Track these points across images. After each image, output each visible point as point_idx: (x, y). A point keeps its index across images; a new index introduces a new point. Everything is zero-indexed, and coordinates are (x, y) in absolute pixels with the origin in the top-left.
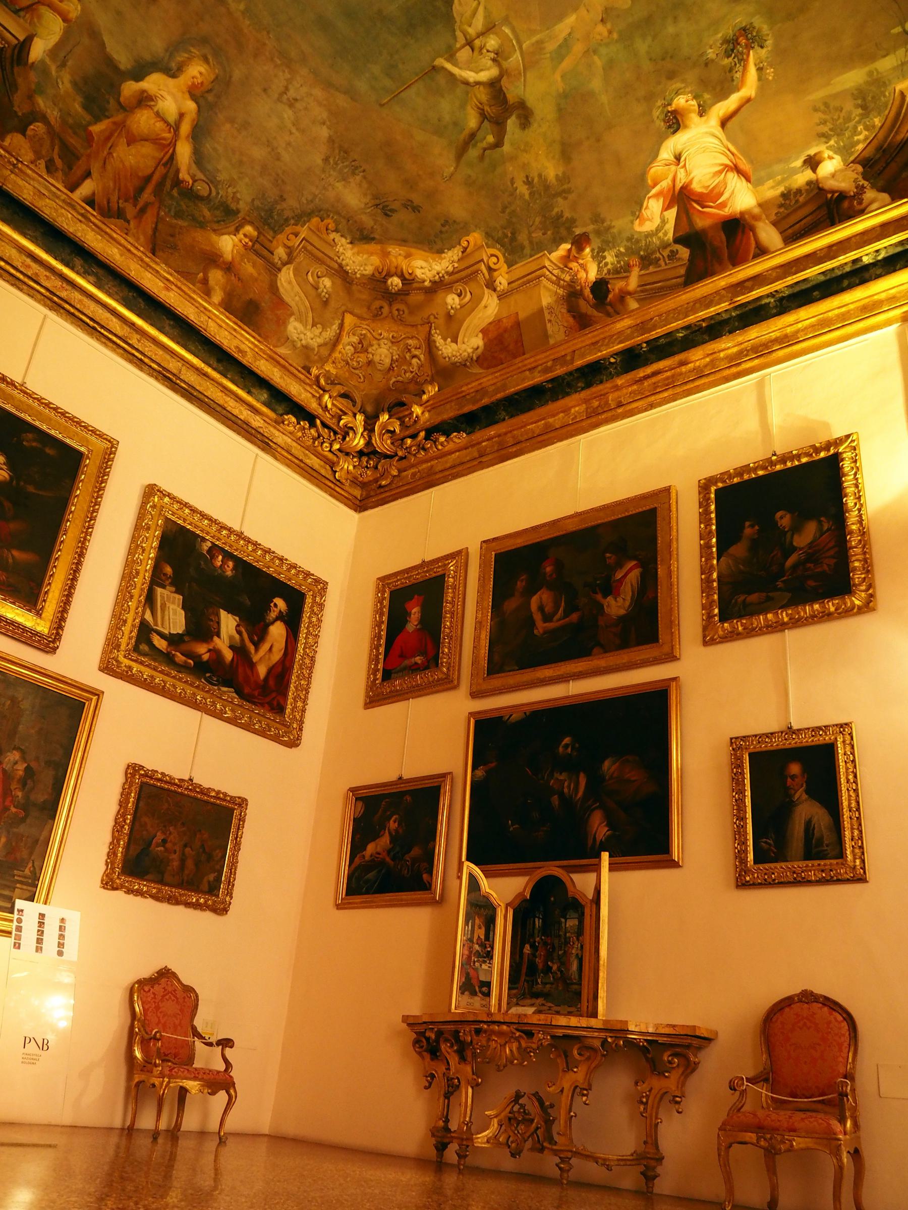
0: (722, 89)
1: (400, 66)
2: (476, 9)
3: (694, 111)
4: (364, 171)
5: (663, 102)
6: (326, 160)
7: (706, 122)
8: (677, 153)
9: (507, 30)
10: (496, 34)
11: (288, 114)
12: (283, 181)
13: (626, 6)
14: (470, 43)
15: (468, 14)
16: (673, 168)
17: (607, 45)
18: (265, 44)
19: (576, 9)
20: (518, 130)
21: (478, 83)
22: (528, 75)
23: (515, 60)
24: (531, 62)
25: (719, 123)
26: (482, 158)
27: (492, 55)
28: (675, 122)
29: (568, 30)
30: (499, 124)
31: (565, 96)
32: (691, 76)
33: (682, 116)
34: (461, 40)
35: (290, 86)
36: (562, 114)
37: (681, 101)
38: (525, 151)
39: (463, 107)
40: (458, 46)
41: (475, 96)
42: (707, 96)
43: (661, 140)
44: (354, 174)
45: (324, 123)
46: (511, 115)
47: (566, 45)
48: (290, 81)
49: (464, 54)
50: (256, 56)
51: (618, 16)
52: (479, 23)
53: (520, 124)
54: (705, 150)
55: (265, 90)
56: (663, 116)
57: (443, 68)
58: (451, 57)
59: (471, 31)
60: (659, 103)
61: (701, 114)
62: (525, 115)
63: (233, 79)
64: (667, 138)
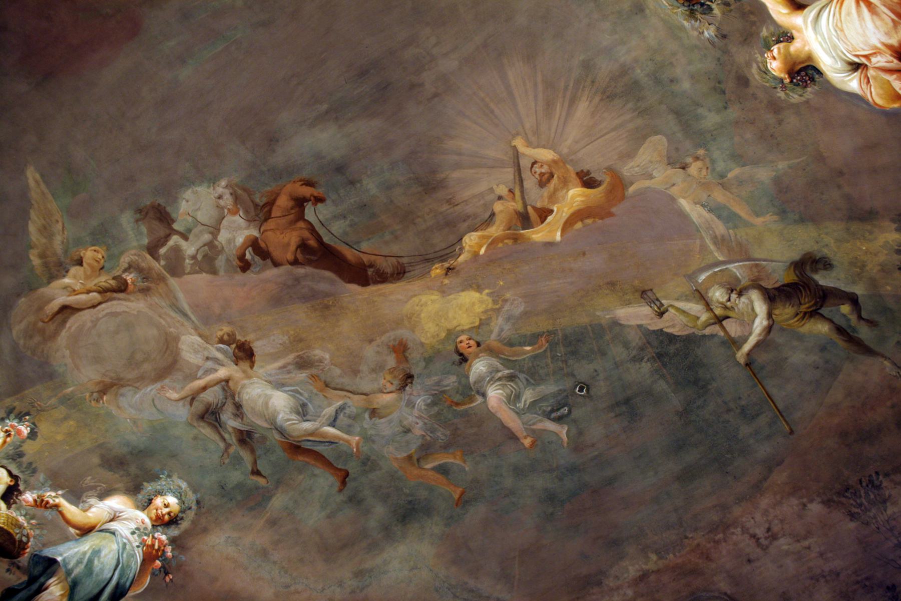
0: (752, 13)
1: (743, 403)
2: (678, 309)
3: (787, 49)
4: (877, 473)
5: (779, 90)
6: (852, 516)
7: (799, 30)
8: (849, 68)
9: (702, 277)
10: (707, 289)
11: (784, 543)
12: (867, 579)
13: (664, 139)
14: (719, 320)
15: (682, 318)
16: (871, 73)
17: (713, 162)
18: (698, 545)
19: (673, 199)
20: (834, 274)
21: (770, 315)
22: (757, 256)
23: (737, 269)
24: (741, 252)
25: (799, 12)
26: (872, 323)
27: (734, 296)
28: (805, 72)
29: (699, 208)
30: (825, 296)
31: (782, 213)
32: (740, 55)
33: (794, 64)
34: (716, 329)
35: (751, 531)
36: (808, 217)
37: (775, 66)
38: (863, 267)
39: (800, 338)
40: (722, 334)
41: (787, 320)
42: (764, 33)
43: (830, 90)
44: (879, 487)
45: (805, 505)
46: (814, 280)
47: (717, 210)
48: (745, 530)
49: (733, 328)
50: (709, 559)
51: (677, 149)
52: (694, 307)
53: (825, 269)
54: (839, 29)
55: (749, 561)
56: (799, 90)
57: (749, 354)
58: (735, 343)
59: (704, 317)
60: (781, 95)
61: (791, 39)
62: (809, 264)
63: (729, 592)
64: (828, 82)
